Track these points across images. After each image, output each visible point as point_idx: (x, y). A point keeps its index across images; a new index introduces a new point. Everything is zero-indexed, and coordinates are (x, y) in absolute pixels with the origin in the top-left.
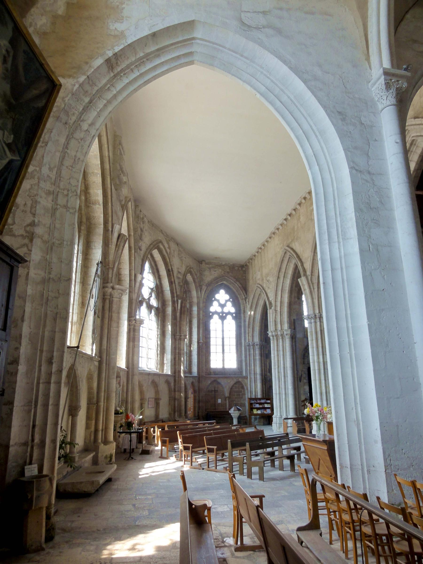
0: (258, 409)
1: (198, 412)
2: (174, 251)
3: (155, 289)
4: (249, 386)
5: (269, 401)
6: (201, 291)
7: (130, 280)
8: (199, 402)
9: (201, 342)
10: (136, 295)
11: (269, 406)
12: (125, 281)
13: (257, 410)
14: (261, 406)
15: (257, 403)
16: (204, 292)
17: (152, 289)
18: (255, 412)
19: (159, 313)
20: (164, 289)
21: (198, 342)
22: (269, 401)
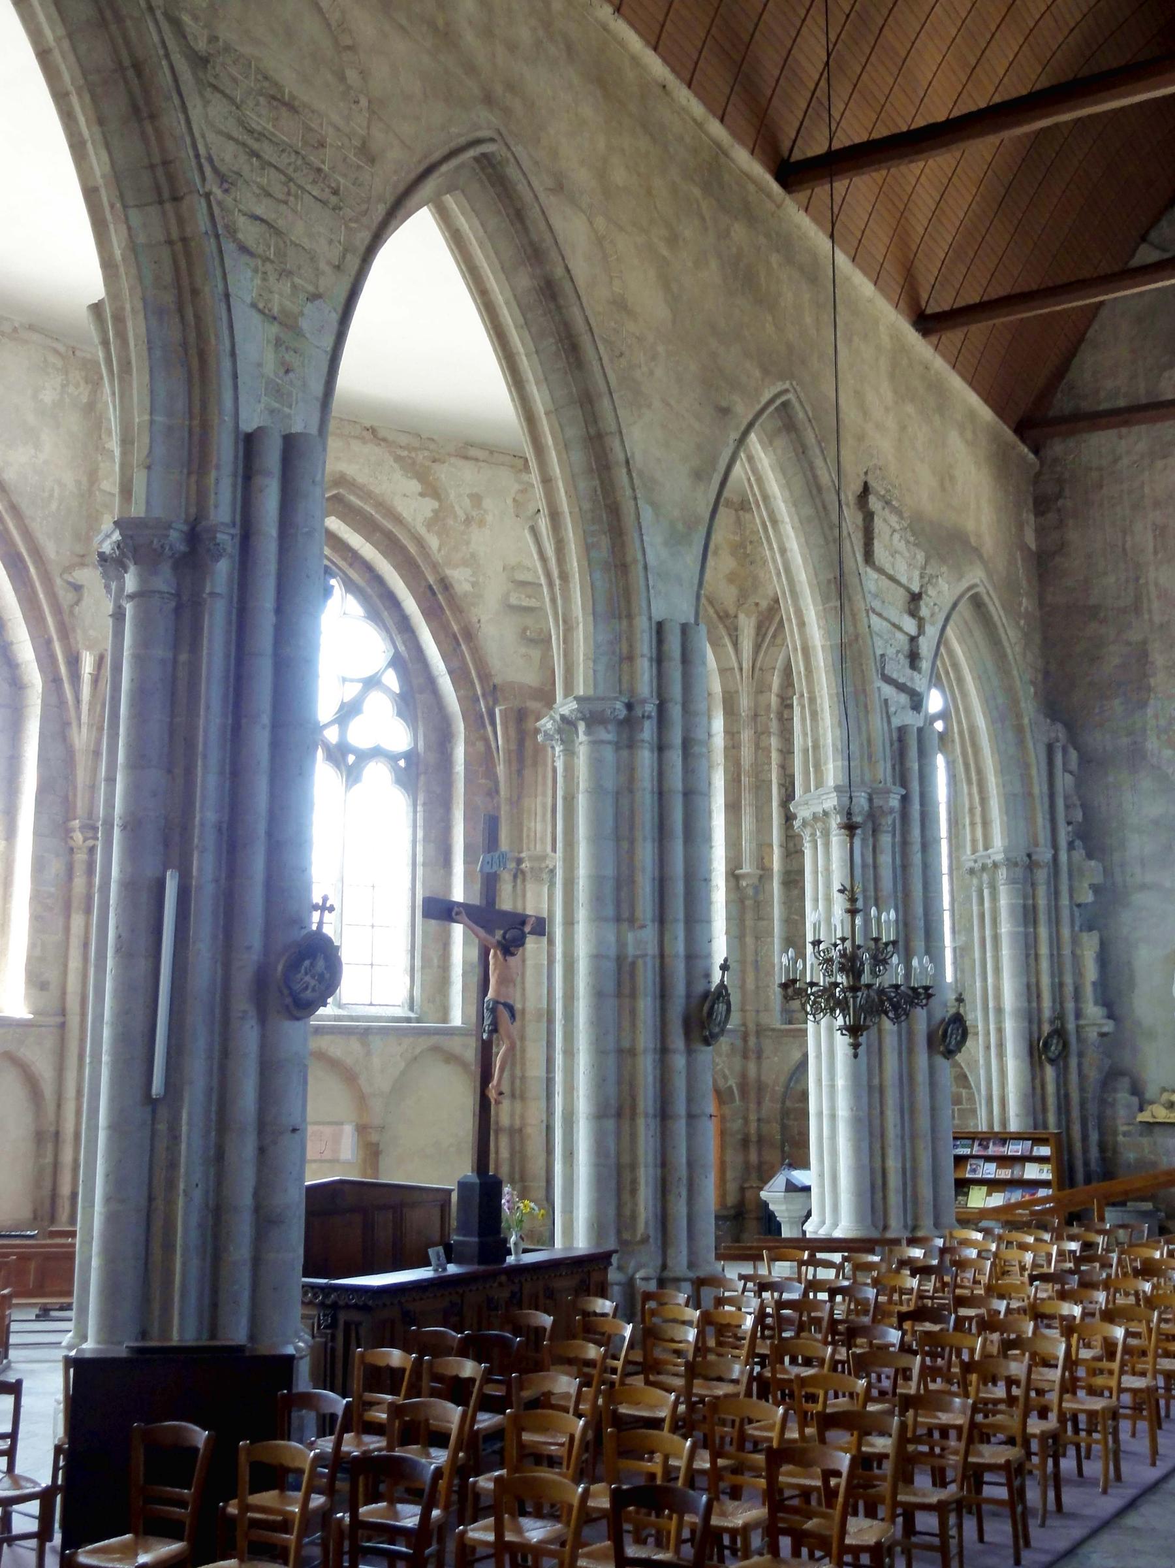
0: (994, 1185)
1: (742, 1190)
2: (476, 499)
3: (391, 680)
4: (982, 1072)
5: (1045, 1151)
6: (735, 644)
7: (53, 681)
8: (745, 1143)
9: (743, 876)
10: (84, 730)
11: (1043, 1173)
12: (33, 685)
13: (989, 1194)
14: (1005, 1174)
15: (989, 1159)
16: (747, 645)
17: (372, 683)
18: (978, 1199)
19: (418, 776)
20: (436, 673)
21: (733, 876)
22: (1045, 1151)
